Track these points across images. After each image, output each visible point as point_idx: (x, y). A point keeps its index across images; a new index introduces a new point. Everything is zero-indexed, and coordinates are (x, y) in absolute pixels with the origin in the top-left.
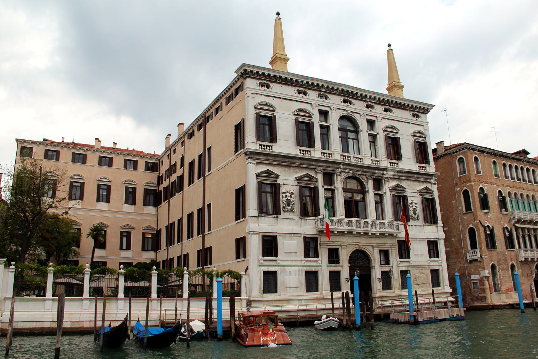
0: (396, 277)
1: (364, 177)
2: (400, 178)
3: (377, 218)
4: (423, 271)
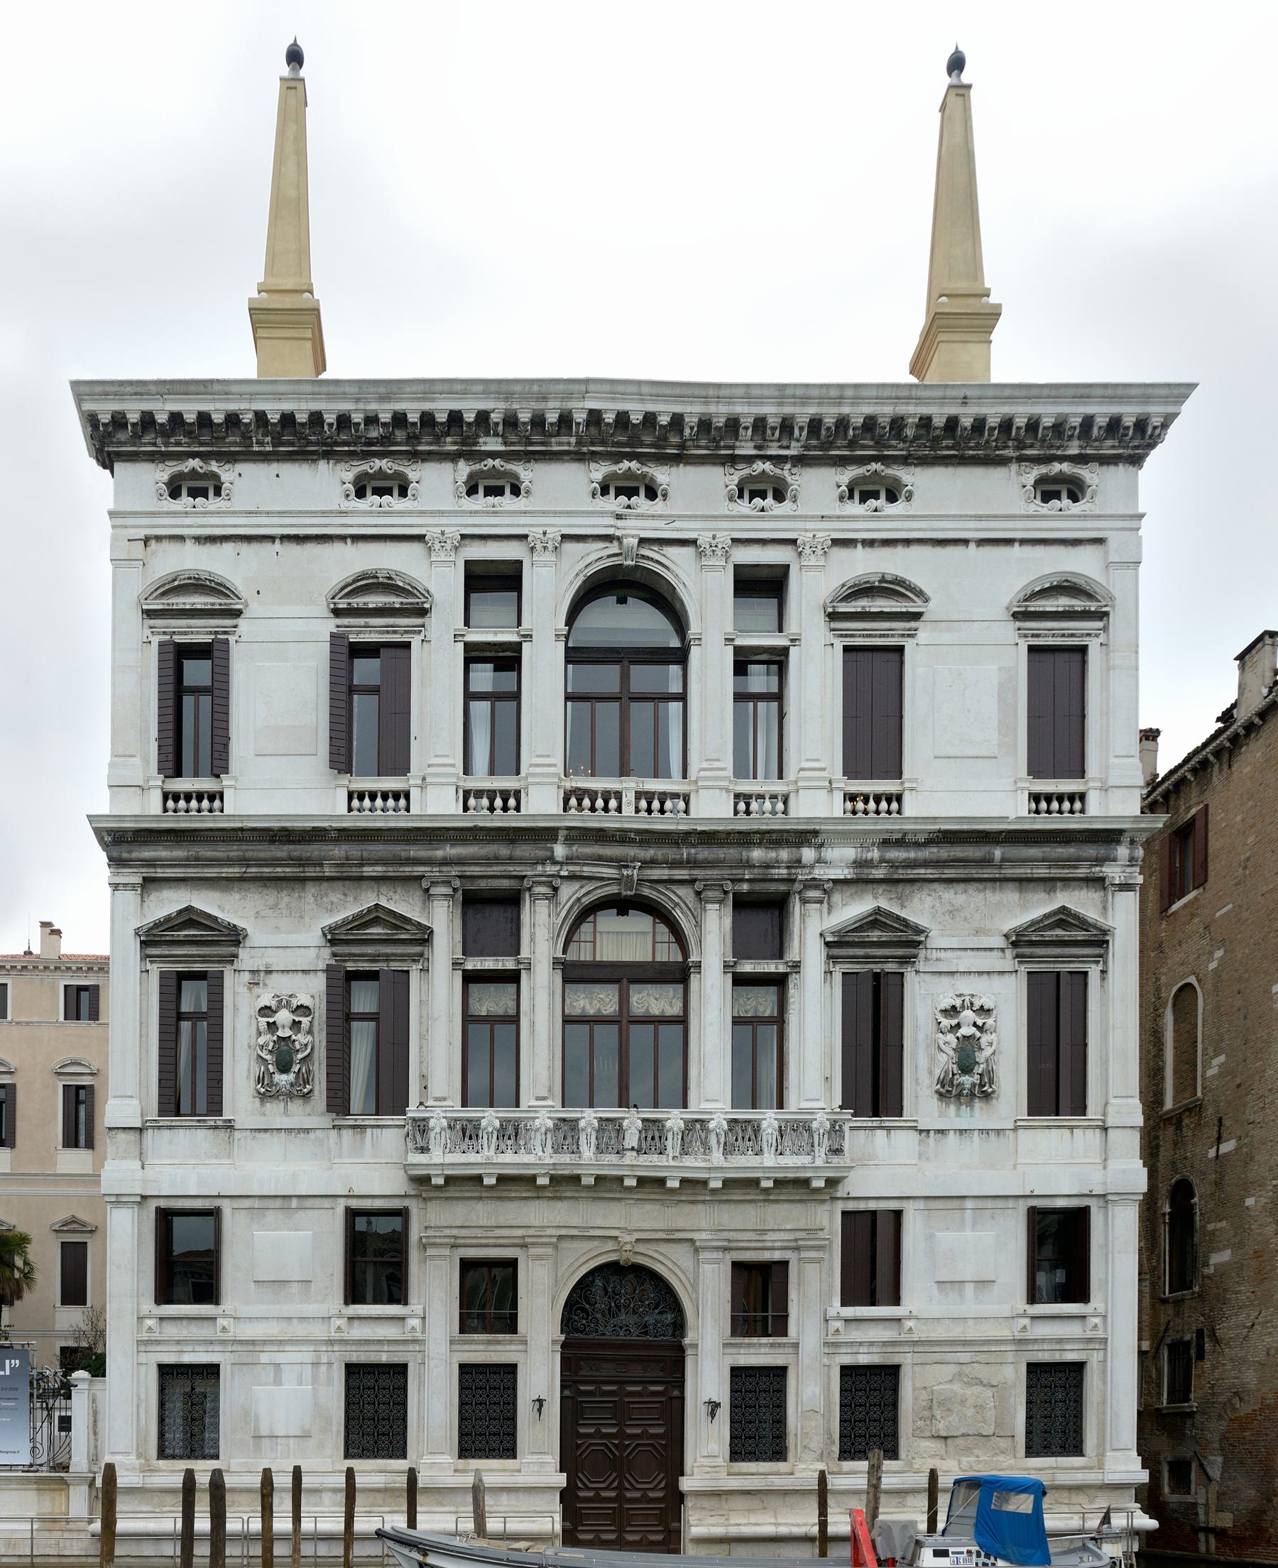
1: (686, 893)
2: (901, 873)
4: (981, 1372)
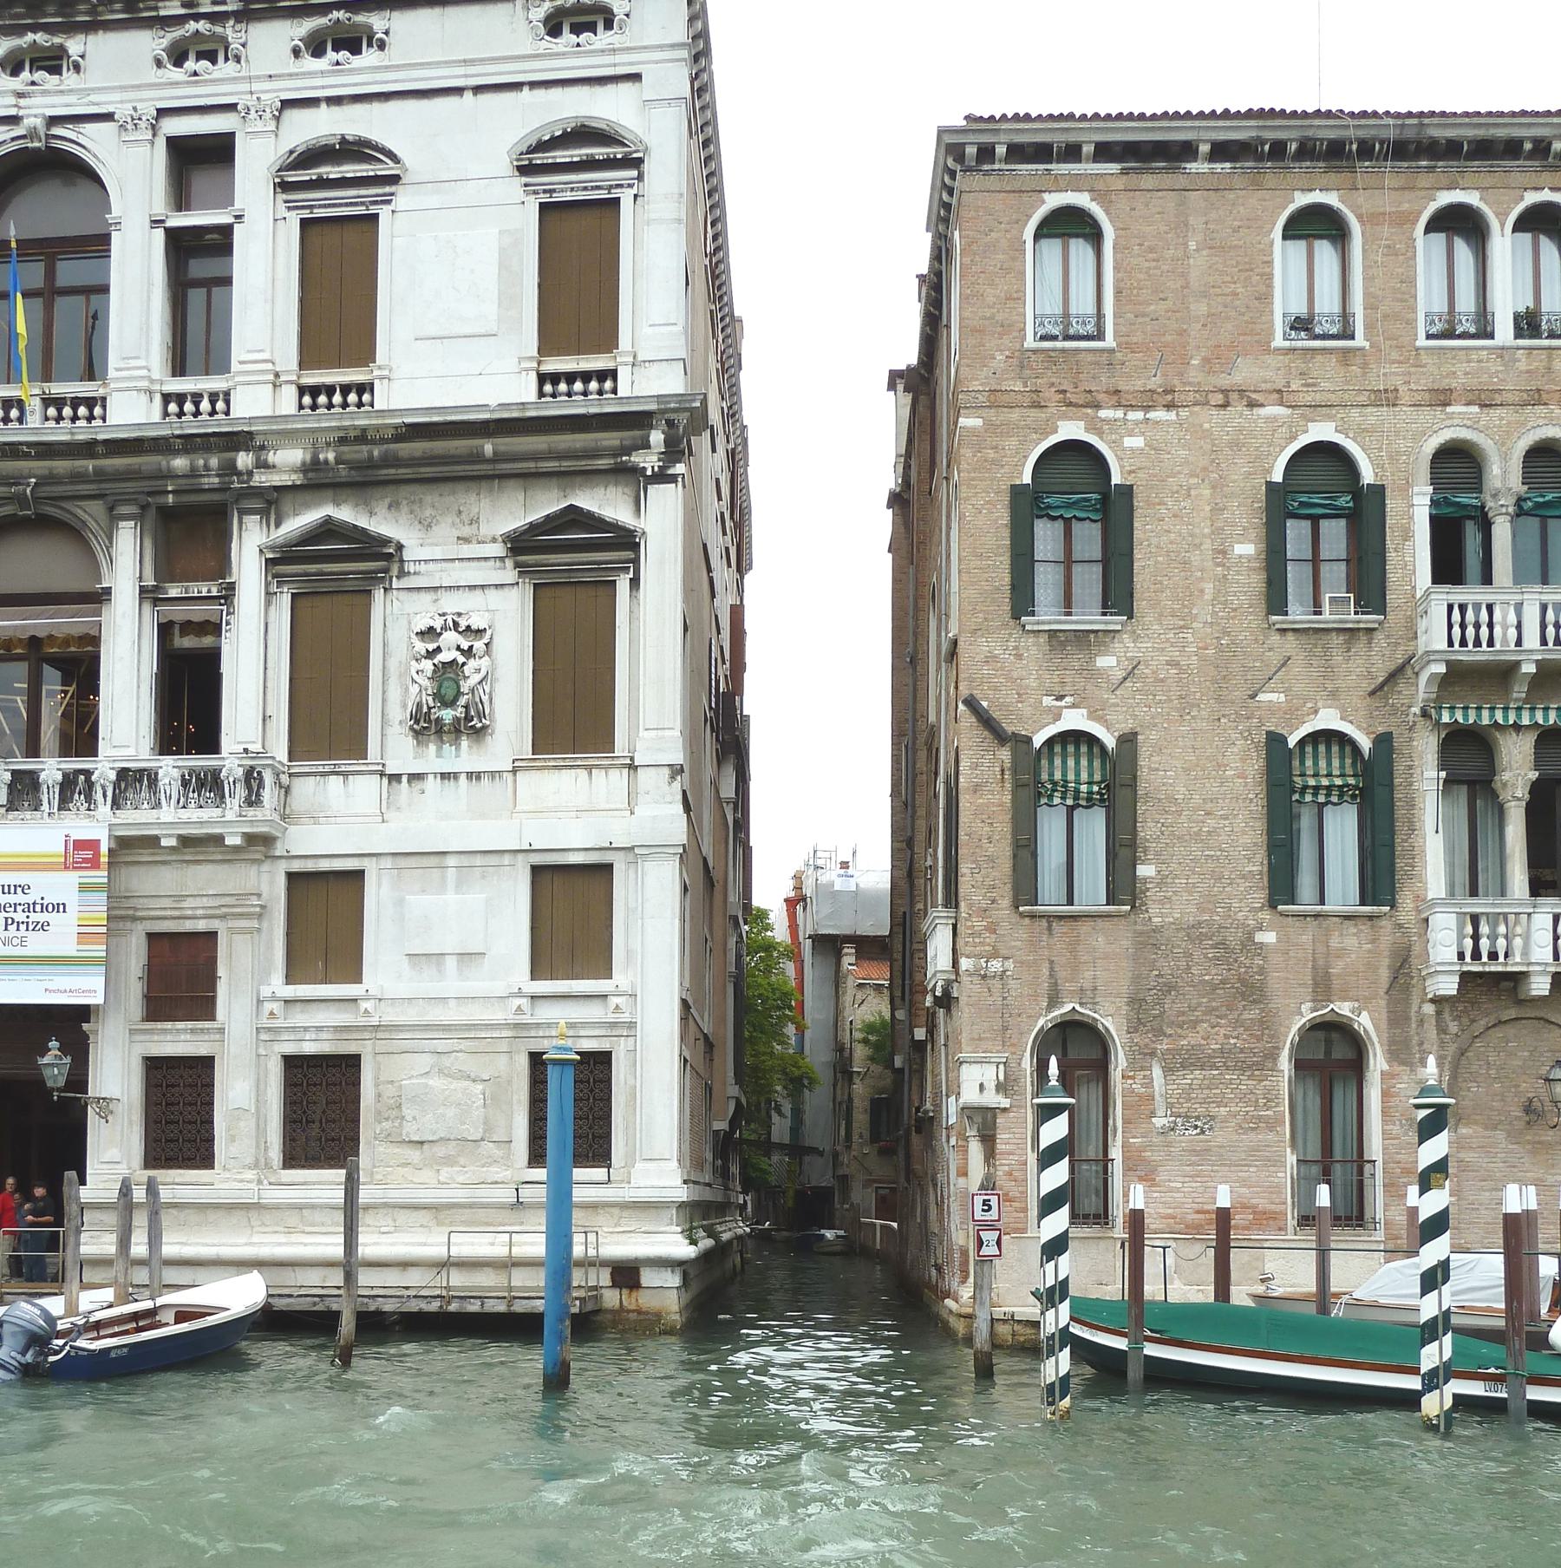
0: (247, 1102)
3: (168, 742)
